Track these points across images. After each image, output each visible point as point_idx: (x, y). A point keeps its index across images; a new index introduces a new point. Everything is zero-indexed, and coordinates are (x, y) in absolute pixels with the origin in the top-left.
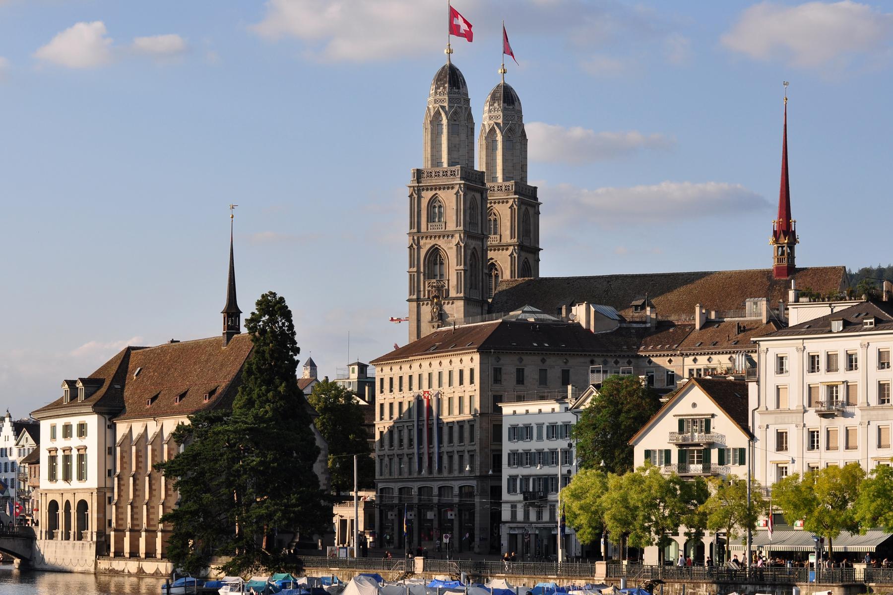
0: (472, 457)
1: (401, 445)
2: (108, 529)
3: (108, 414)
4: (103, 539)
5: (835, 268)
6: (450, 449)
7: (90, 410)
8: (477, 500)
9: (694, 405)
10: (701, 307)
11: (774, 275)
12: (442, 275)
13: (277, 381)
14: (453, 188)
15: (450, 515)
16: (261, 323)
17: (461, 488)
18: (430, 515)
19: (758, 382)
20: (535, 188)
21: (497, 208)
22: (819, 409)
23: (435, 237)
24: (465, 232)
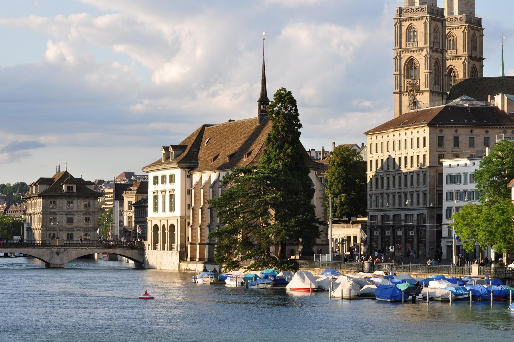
0: (425, 194)
2: (187, 243)
4: (184, 249)
6: (412, 190)
7: (176, 166)
12: (415, 76)
13: (286, 145)
14: (422, 19)
15: (411, 233)
16: (276, 108)
17: (418, 215)
20: (480, 19)
21: (454, 32)
23: (411, 51)
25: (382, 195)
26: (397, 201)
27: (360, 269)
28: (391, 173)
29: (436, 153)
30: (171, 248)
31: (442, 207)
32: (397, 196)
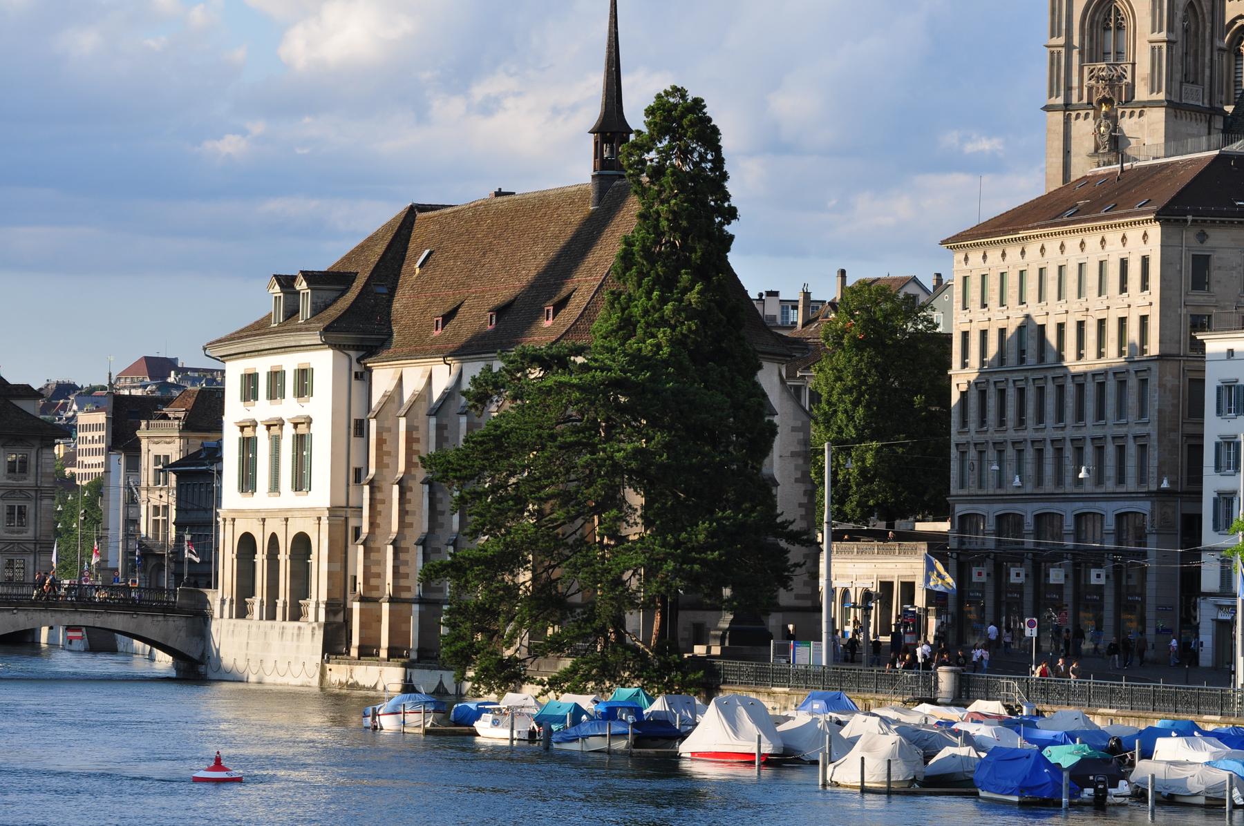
0: (1143, 448)
1: (1002, 422)
2: (349, 596)
3: (356, 348)
6: (1098, 432)
7: (316, 338)
12: (1119, 53)
13: (685, 278)
15: (1096, 577)
16: (653, 154)
17: (1120, 517)
18: (1056, 576)
25: (1000, 447)
26: (1049, 469)
27: (920, 693)
28: (1031, 376)
29: (1184, 311)
30: (296, 614)
31: (1201, 493)
32: (1049, 453)
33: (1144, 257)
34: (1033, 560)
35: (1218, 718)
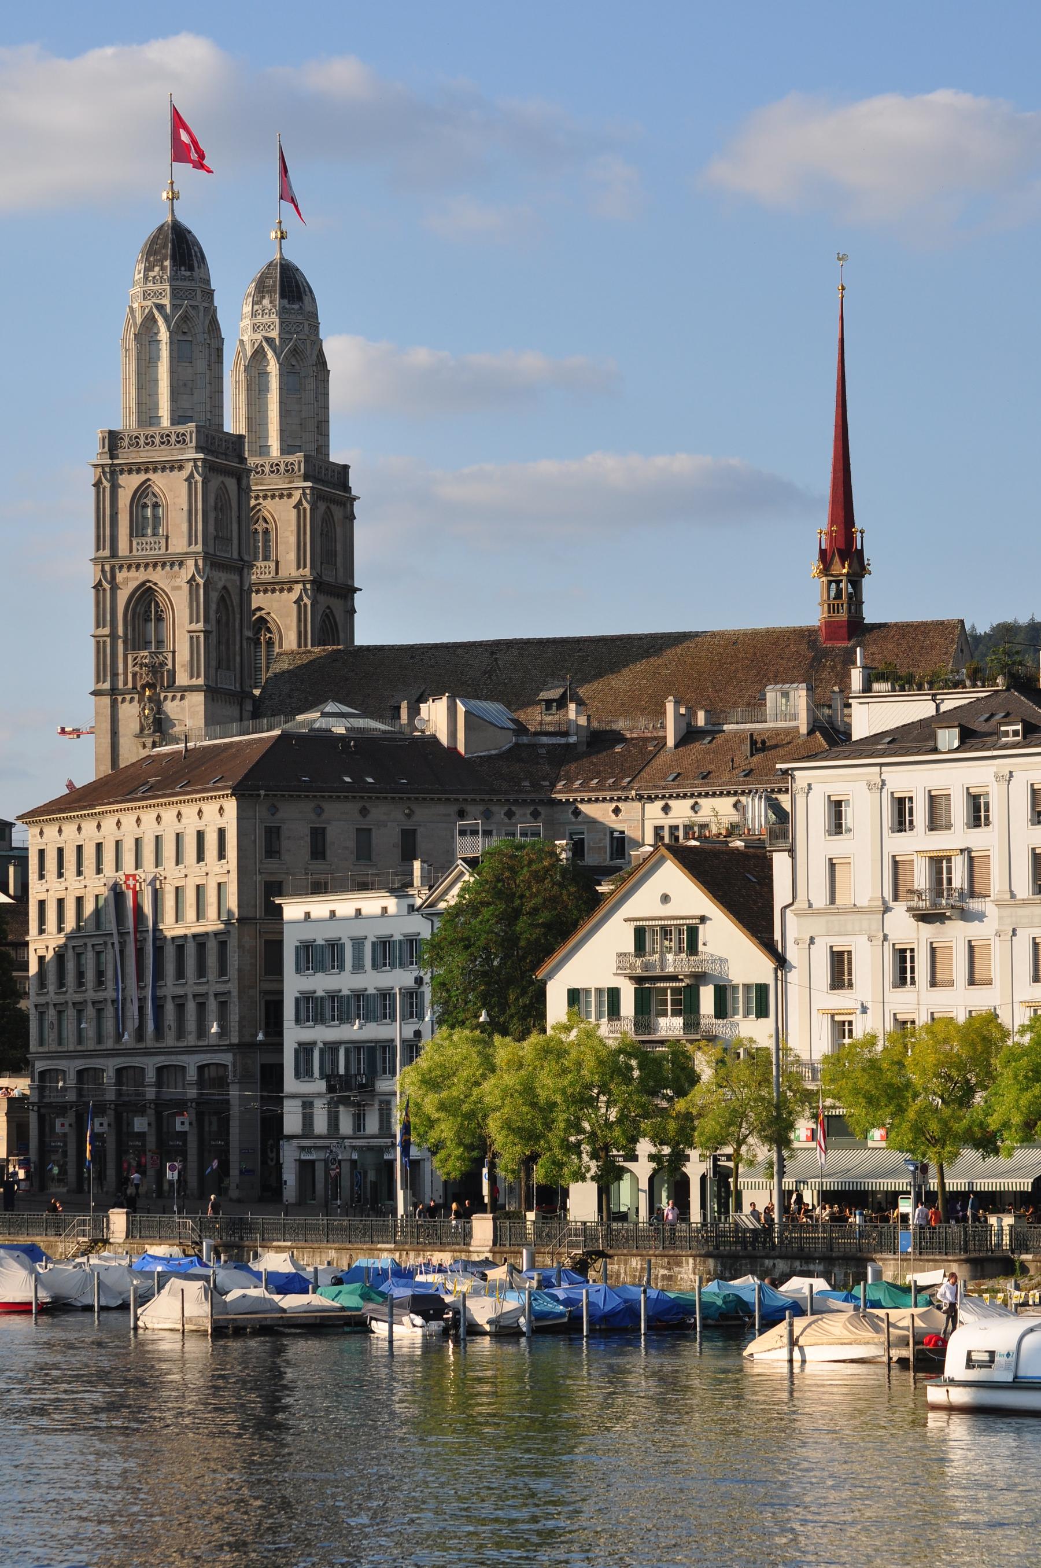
0: (223, 1005)
5: (942, 623)
6: (179, 991)
8: (234, 1092)
9: (665, 899)
10: (677, 703)
11: (821, 638)
12: (160, 643)
14: (181, 468)
15: (182, 1123)
17: (201, 1069)
18: (140, 1124)
19: (792, 851)
20: (346, 468)
22: (913, 904)
23: (147, 566)
24: (206, 556)
25: (79, 1008)
29: (259, 878)
33: (199, 832)
34: (115, 1110)
35: (392, 1246)
